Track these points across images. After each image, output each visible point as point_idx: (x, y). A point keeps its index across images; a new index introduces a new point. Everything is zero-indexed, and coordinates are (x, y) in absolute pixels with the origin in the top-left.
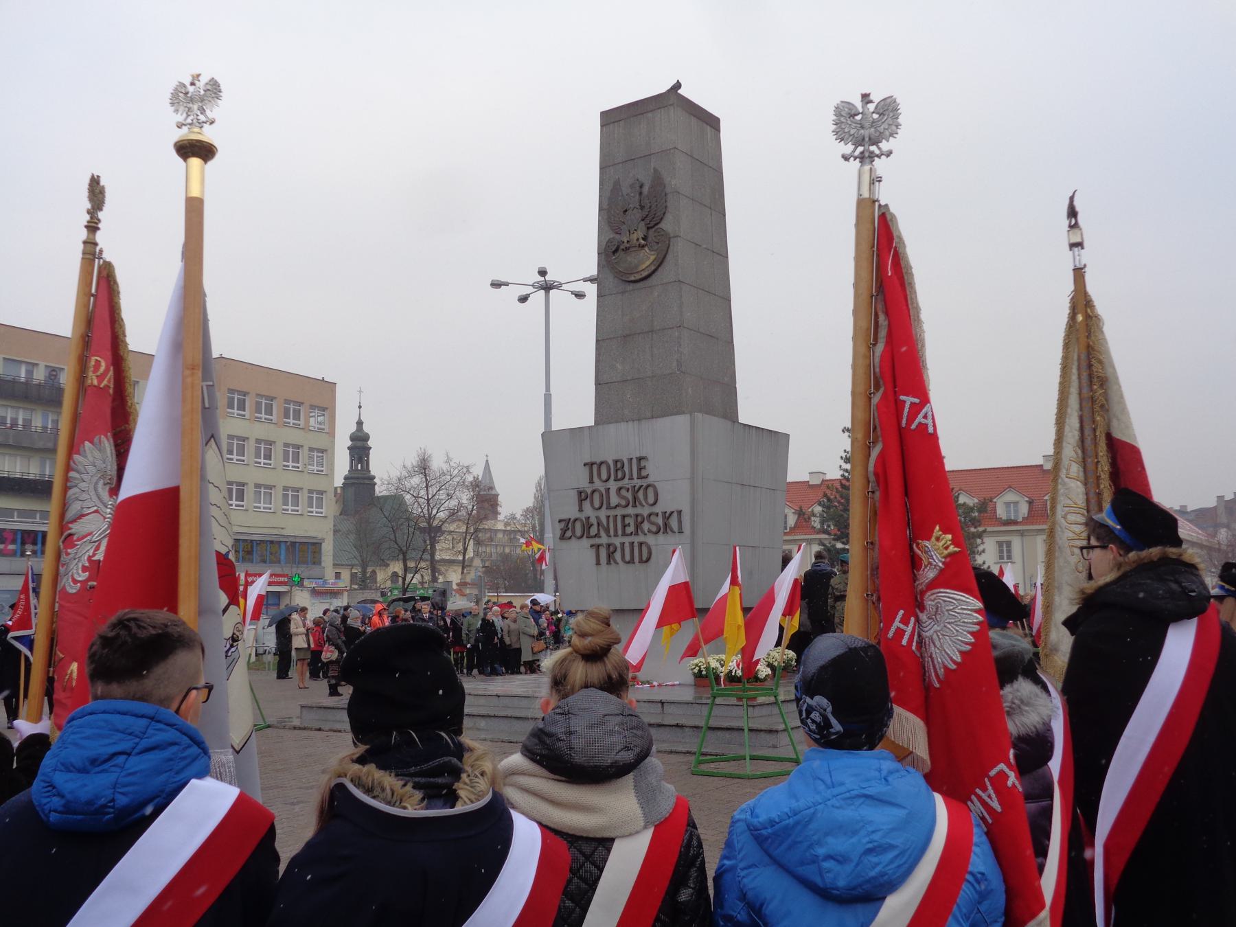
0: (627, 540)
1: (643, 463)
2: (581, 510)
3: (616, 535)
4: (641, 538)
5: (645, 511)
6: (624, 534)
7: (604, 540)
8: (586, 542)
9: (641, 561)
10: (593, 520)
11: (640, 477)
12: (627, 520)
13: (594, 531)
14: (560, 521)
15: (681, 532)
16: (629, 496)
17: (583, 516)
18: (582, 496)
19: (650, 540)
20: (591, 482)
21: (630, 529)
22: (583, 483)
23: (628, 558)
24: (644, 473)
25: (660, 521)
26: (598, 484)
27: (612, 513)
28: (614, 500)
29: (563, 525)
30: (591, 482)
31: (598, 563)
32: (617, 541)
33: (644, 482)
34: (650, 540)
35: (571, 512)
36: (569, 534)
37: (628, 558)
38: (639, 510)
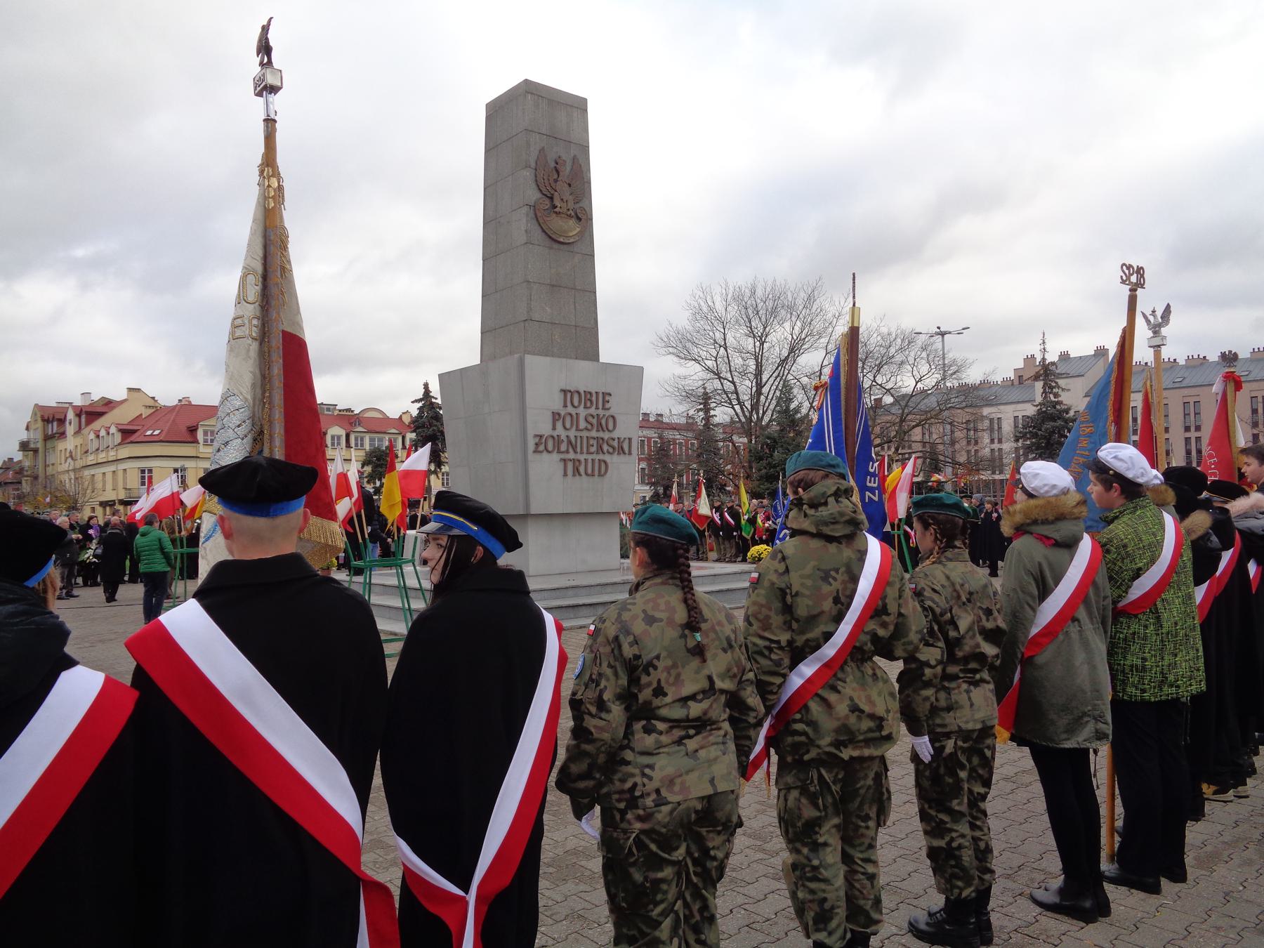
0: (590, 457)
1: (607, 398)
2: (554, 428)
3: (582, 453)
4: (601, 457)
5: (606, 436)
6: (588, 453)
7: (571, 455)
8: (556, 457)
9: (600, 475)
10: (563, 437)
11: (604, 408)
12: (592, 442)
13: (563, 447)
14: (536, 436)
15: (630, 453)
16: (594, 421)
17: (555, 434)
18: (556, 416)
19: (607, 458)
20: (565, 406)
21: (593, 449)
22: (557, 405)
23: (590, 471)
24: (607, 406)
25: (615, 444)
26: (570, 409)
27: (579, 434)
28: (583, 424)
29: (537, 440)
30: (565, 406)
31: (565, 474)
32: (582, 458)
33: (607, 413)
34: (607, 458)
35: (546, 429)
36: (542, 448)
37: (590, 471)
38: (601, 434)
